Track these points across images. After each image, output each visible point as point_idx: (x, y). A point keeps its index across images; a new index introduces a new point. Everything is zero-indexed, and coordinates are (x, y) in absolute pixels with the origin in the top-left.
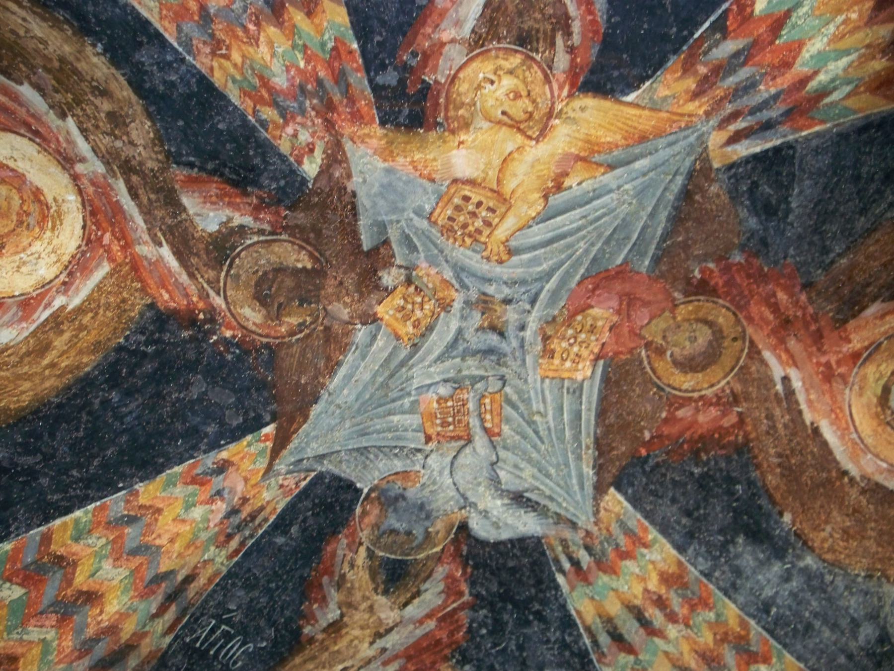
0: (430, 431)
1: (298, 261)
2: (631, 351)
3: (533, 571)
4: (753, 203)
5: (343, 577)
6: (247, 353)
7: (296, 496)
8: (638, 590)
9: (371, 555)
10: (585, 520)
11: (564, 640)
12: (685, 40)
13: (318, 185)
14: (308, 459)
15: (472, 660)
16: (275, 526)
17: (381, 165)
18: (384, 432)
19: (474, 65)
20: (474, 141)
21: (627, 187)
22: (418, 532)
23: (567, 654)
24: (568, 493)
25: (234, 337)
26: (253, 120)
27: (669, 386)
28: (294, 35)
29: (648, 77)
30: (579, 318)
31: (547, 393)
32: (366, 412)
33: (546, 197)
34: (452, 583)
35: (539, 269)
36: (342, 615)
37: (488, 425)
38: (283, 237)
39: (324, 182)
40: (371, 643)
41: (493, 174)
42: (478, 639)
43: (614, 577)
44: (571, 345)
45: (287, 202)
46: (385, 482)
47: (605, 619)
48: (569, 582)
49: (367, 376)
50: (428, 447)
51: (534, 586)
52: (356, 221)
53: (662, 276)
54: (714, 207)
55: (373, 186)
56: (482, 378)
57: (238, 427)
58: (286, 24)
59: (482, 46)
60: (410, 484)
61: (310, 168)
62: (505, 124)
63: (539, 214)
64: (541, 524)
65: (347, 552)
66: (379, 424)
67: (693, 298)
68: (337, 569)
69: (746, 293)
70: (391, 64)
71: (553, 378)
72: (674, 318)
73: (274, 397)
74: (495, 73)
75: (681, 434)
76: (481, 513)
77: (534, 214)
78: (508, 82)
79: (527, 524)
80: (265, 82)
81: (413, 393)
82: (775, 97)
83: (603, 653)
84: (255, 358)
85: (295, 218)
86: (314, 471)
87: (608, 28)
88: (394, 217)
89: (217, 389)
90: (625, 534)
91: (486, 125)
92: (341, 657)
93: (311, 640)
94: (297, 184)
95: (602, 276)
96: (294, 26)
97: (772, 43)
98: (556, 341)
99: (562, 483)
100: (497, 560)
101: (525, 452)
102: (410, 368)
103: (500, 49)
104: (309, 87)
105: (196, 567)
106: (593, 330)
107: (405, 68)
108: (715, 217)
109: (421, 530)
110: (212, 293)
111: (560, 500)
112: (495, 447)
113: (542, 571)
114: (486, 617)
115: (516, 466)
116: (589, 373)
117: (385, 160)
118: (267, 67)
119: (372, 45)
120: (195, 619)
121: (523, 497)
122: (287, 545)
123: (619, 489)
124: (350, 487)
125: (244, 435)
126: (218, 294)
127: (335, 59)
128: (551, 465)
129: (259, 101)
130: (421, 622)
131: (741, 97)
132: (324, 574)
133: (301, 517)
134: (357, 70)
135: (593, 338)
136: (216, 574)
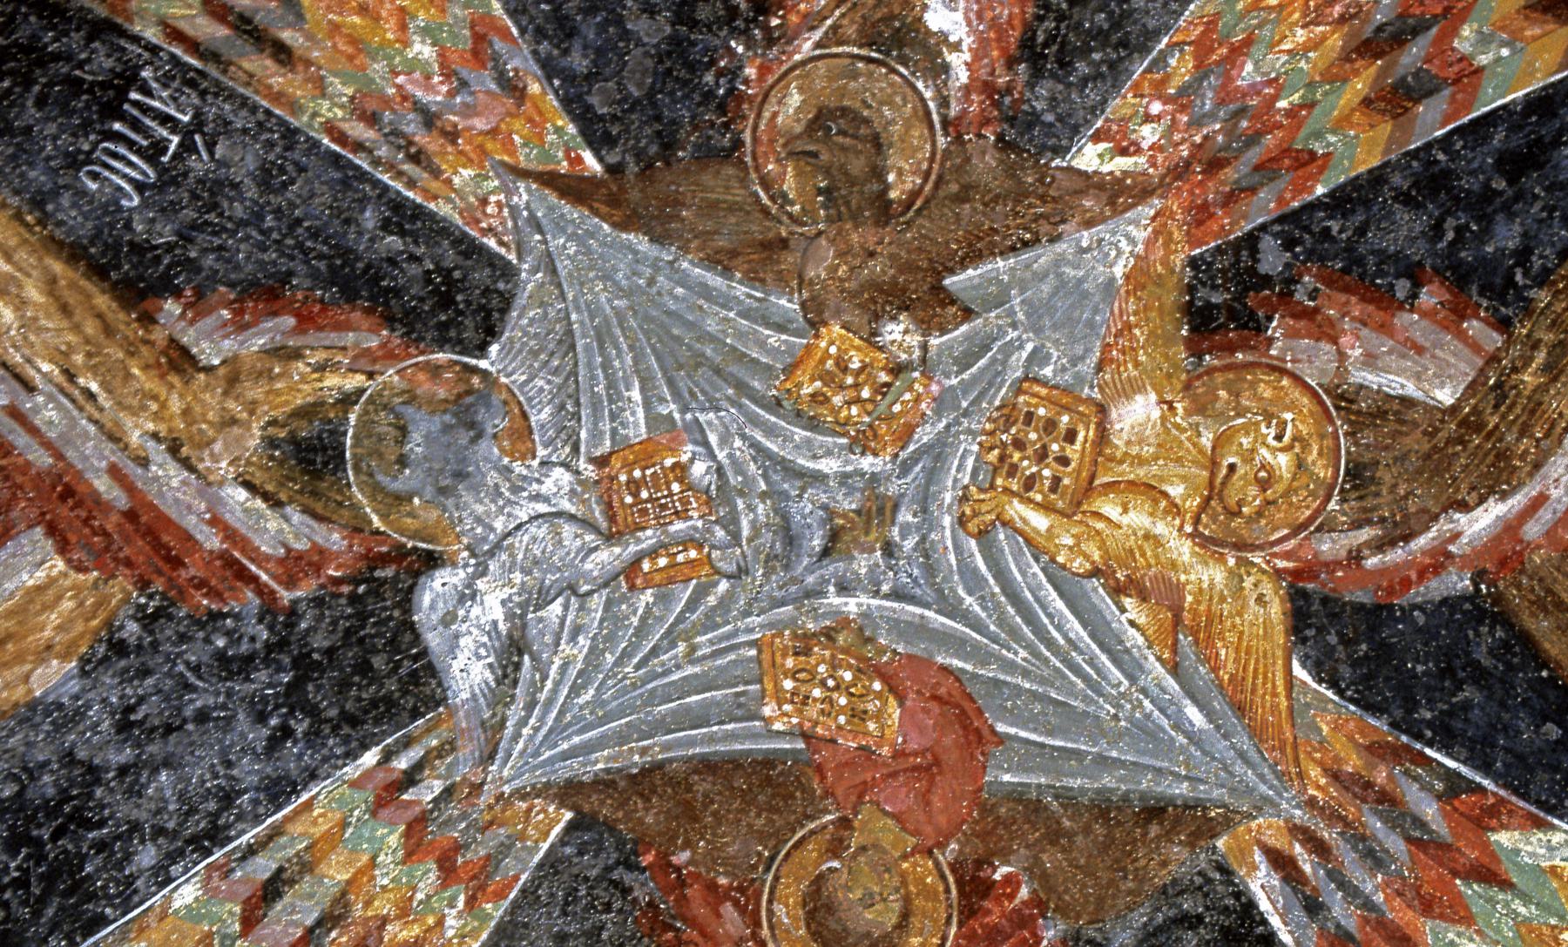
0: (616, 463)
1: (900, 173)
3: (374, 703)
4: (1159, 929)
5: (297, 354)
6: (722, 109)
7: (465, 234)
8: (384, 907)
9: (347, 400)
10: (504, 774)
11: (241, 793)
12: (1418, 737)
13: (1058, 174)
14: (545, 242)
15: (151, 633)
16: (399, 205)
17: (1119, 271)
18: (607, 377)
20: (1177, 426)
21: (1147, 703)
22: (407, 479)
23: (212, 806)
24: (551, 731)
25: (746, 82)
26: (1162, 46)
27: (776, 878)
28: (1331, 82)
29: (1340, 693)
30: (877, 686)
31: (732, 657)
32: (646, 333)
33: (1095, 572)
34: (310, 564)
35: (961, 592)
36: (209, 369)
37: (646, 566)
38: (942, 141)
40: (155, 436)
41: (1127, 472)
42: (201, 634)
43: (401, 853)
44: (823, 683)
45: (1011, 135)
46: (504, 396)
47: (307, 857)
48: (368, 774)
49: (711, 326)
50: (582, 464)
51: (343, 712)
52: (1002, 253)
53: (986, 810)
54: (1142, 862)
55: (1076, 267)
56: (736, 536)
57: (589, 108)
58: (1348, 66)
59: (1338, 408)
61: (1089, 157)
62: (1213, 475)
63: (1063, 567)
64: (474, 695)
65: (351, 353)
67: (951, 879)
70: (1296, 256)
71: (760, 662)
72: (905, 857)
73: (650, 166)
74: (1294, 439)
75: (692, 922)
76: (469, 586)
78: (1283, 461)
79: (468, 672)
80: (1239, 52)
81: (689, 416)
82: (1368, 905)
83: (233, 870)
85: (984, 153)
86: (520, 257)
87: (1402, 609)
88: (1021, 316)
89: (649, 63)
90: (488, 857)
91: (1206, 440)
92: (117, 383)
93: (148, 319)
95: (966, 704)
96: (1345, 80)
97: (1455, 874)
98: (827, 653)
99: (568, 717)
100: (379, 635)
101: (611, 639)
102: (733, 403)
103: (1338, 438)
104: (1244, 124)
105: (308, 63)
106: (858, 715)
107: (1290, 281)
108: (1124, 869)
109: (413, 484)
110: (817, 35)
111: (532, 721)
113: (377, 721)
114: (253, 639)
115: (577, 631)
116: (778, 726)
117: (1127, 277)
118: (1272, 45)
119: (1323, 220)
120: (192, 80)
121: (520, 653)
123: (571, 827)
124: (491, 332)
125: (575, 119)
126: (818, 45)
127: (1296, 159)
128: (597, 689)
129: (1203, 47)
130: (215, 521)
131: (1355, 848)
132: (298, 315)
134: (1281, 201)
135: (842, 719)
136: (295, 107)
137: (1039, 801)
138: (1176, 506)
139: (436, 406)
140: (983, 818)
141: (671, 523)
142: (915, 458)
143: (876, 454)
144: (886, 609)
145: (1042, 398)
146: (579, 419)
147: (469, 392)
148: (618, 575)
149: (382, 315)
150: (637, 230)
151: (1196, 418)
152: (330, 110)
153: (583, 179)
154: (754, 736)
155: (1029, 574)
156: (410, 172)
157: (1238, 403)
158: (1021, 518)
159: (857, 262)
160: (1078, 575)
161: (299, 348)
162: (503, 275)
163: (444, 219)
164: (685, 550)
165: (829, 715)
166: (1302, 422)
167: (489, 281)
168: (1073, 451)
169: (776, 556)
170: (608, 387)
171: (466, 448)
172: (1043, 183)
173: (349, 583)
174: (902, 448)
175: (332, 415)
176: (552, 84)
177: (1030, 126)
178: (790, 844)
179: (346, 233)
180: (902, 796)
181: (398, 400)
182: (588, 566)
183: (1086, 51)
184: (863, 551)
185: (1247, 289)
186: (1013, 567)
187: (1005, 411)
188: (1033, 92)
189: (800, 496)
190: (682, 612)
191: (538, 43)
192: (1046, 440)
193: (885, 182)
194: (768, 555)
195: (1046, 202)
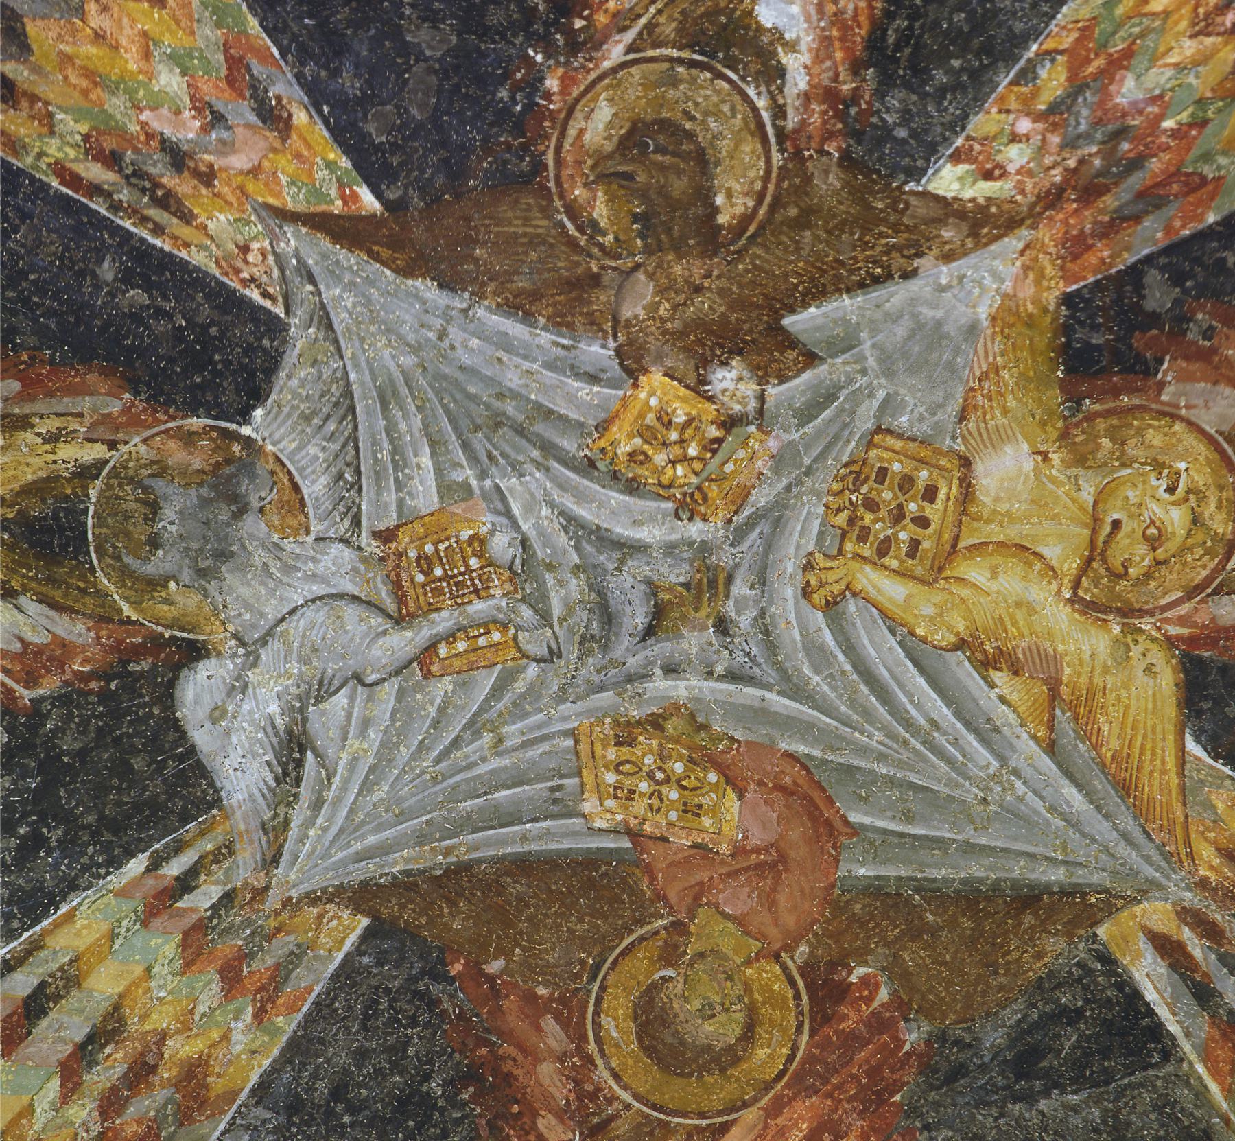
2: (660, 896)
5: (24, 423)
9: (86, 473)
13: (913, 201)
14: (320, 294)
16: (143, 253)
17: (983, 312)
18: (391, 441)
19: (1201, 448)
20: (1053, 480)
22: (162, 562)
27: (603, 988)
32: (438, 393)
33: (961, 645)
35: (807, 671)
37: (443, 651)
39: (922, 211)
41: (993, 532)
45: (858, 151)
46: (271, 465)
49: (513, 380)
50: (365, 540)
52: (848, 290)
53: (838, 908)
55: (936, 307)
57: (365, 136)
60: (275, 518)
61: (948, 180)
63: (924, 640)
65: (88, 420)
66: (410, 425)
67: (801, 984)
68: (39, 407)
69: (835, 1080)
70: (1186, 292)
71: (577, 754)
72: (748, 962)
73: (437, 199)
74: (1188, 492)
77: (920, 631)
78: (1176, 518)
84: (509, 147)
86: (287, 312)
88: (871, 362)
91: (1087, 495)
94: (906, 161)
95: (816, 795)
107: (1181, 319)
109: (169, 567)
112: (397, 673)
116: (599, 823)
117: (993, 319)
122: (97, 287)
124: (255, 394)
125: (347, 150)
133: (169, 306)
137: (900, 895)
138: (1052, 569)
139: (190, 478)
140: (834, 917)
141: (470, 602)
142: (750, 524)
143: (705, 520)
144: (721, 691)
145: (897, 453)
146: (360, 489)
147: (229, 461)
148: (410, 662)
149: (123, 376)
150: (423, 276)
151: (1075, 470)
152: (59, 149)
153: (361, 218)
154: (574, 834)
155: (883, 650)
156: (157, 219)
157: (1123, 452)
158: (874, 587)
159: (681, 298)
160: (941, 648)
161: (26, 416)
162: (269, 330)
163: (198, 269)
164: (488, 632)
165: (659, 810)
166: (1199, 472)
167: (252, 339)
168: (933, 512)
169: (593, 637)
170: (393, 454)
171: (228, 524)
172: (895, 210)
173: (98, 679)
174: (736, 512)
175: (69, 491)
176: (320, 112)
177: (879, 143)
178: (618, 951)
179: (80, 286)
180: (744, 896)
181: (146, 472)
182: (376, 652)
183: (943, 58)
184: (694, 628)
185: (1131, 329)
186: (866, 642)
187: (855, 468)
188: (883, 104)
189: (619, 569)
190: (486, 699)
191: (303, 64)
192: (902, 499)
193: (712, 204)
194: (583, 637)
195: (897, 232)
